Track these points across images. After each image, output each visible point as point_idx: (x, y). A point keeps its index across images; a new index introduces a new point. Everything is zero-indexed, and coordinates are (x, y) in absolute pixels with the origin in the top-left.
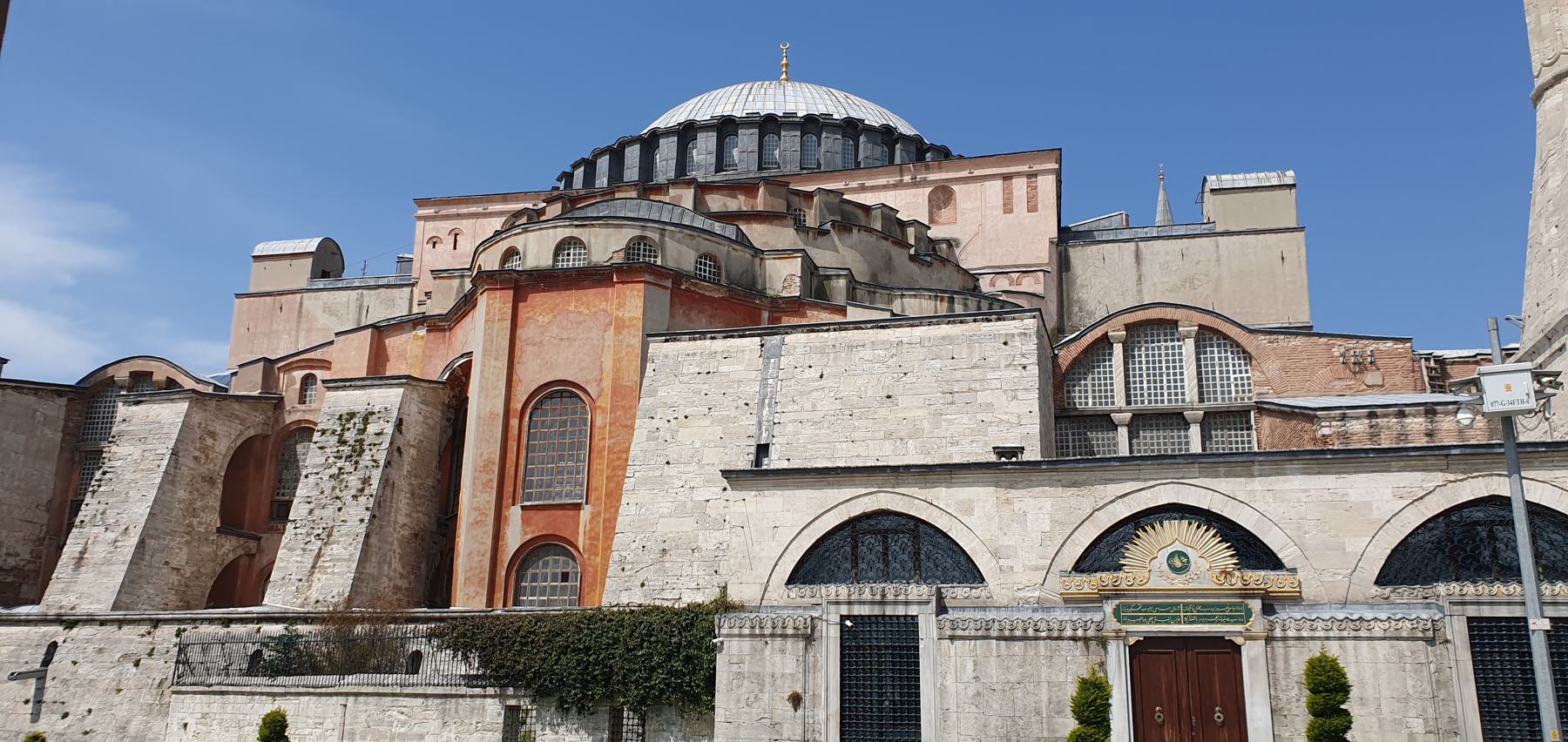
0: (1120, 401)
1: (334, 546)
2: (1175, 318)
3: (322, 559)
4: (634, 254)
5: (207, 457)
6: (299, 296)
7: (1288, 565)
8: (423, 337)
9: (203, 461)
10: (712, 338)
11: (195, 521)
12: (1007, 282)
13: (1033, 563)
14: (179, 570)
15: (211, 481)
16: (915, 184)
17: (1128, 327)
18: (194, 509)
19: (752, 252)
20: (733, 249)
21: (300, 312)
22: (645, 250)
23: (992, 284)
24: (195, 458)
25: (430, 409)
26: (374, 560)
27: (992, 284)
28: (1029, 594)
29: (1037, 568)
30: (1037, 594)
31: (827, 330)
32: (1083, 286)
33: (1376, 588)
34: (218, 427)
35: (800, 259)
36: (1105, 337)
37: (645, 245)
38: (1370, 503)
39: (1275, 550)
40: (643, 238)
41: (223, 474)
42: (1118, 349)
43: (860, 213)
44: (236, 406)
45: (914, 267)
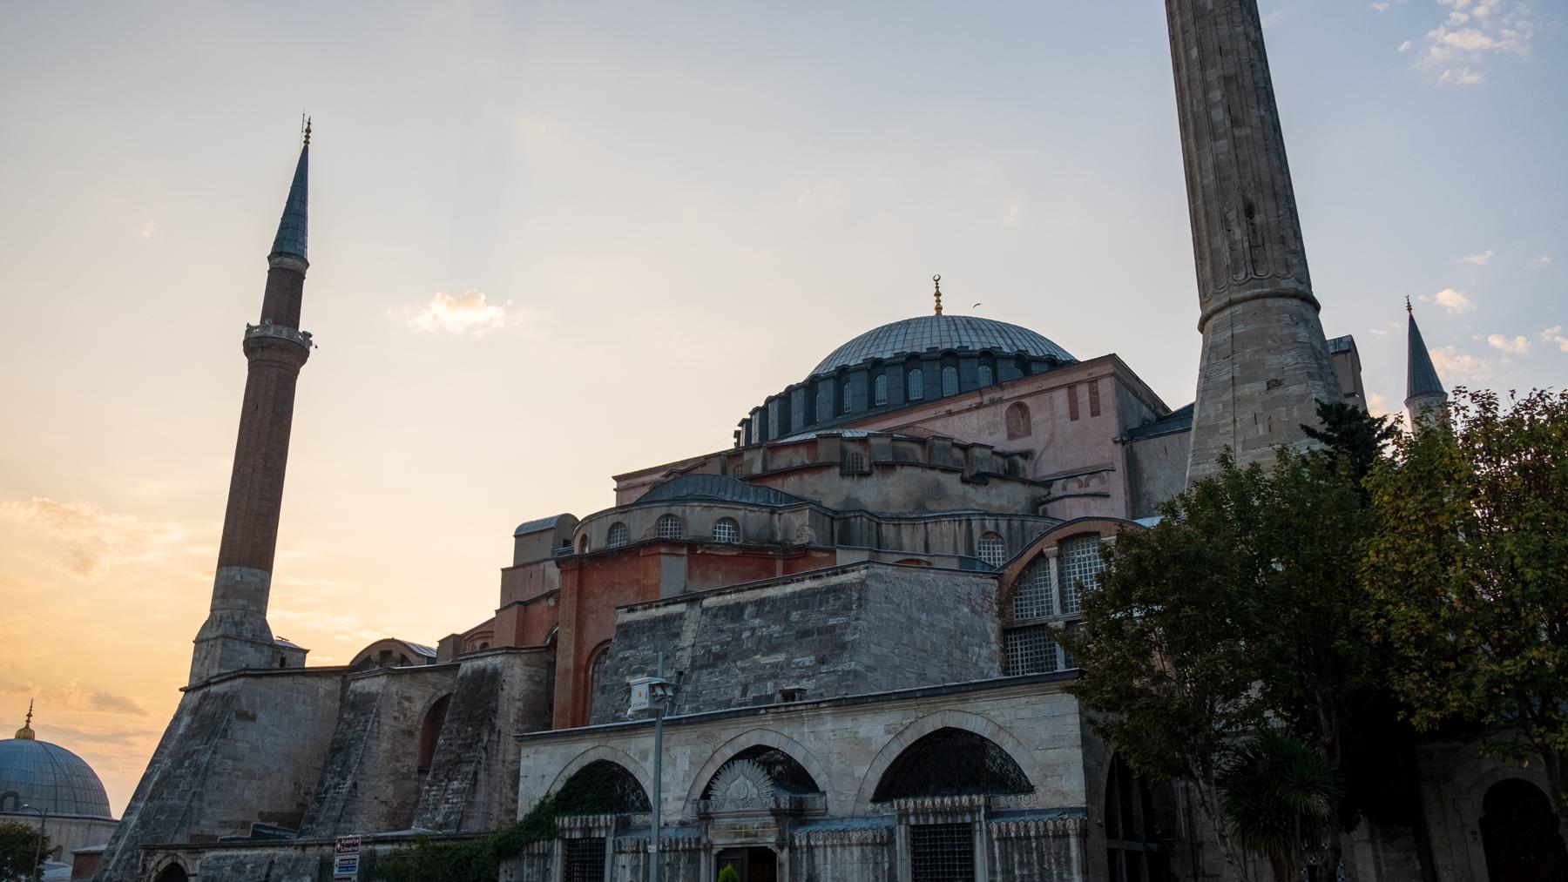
0: (1057, 611)
1: (455, 782)
2: (1096, 530)
3: (447, 792)
4: (663, 529)
5: (405, 716)
6: (542, 565)
7: (821, 789)
8: (553, 607)
9: (401, 719)
10: (658, 606)
11: (398, 765)
12: (1076, 485)
13: (678, 795)
14: (386, 802)
15: (410, 734)
16: (993, 402)
17: (1062, 542)
18: (397, 756)
19: (769, 510)
20: (750, 511)
21: (544, 578)
22: (672, 525)
23: (1064, 488)
24: (395, 718)
25: (534, 669)
26: (483, 791)
27: (1064, 488)
28: (675, 818)
29: (680, 799)
30: (679, 818)
31: (730, 593)
32: (1149, 479)
33: (871, 805)
34: (413, 693)
35: (808, 511)
36: (1041, 555)
37: (672, 520)
38: (870, 739)
39: (813, 776)
40: (668, 516)
41: (420, 727)
42: (1053, 564)
43: (917, 448)
44: (429, 675)
45: (970, 490)
